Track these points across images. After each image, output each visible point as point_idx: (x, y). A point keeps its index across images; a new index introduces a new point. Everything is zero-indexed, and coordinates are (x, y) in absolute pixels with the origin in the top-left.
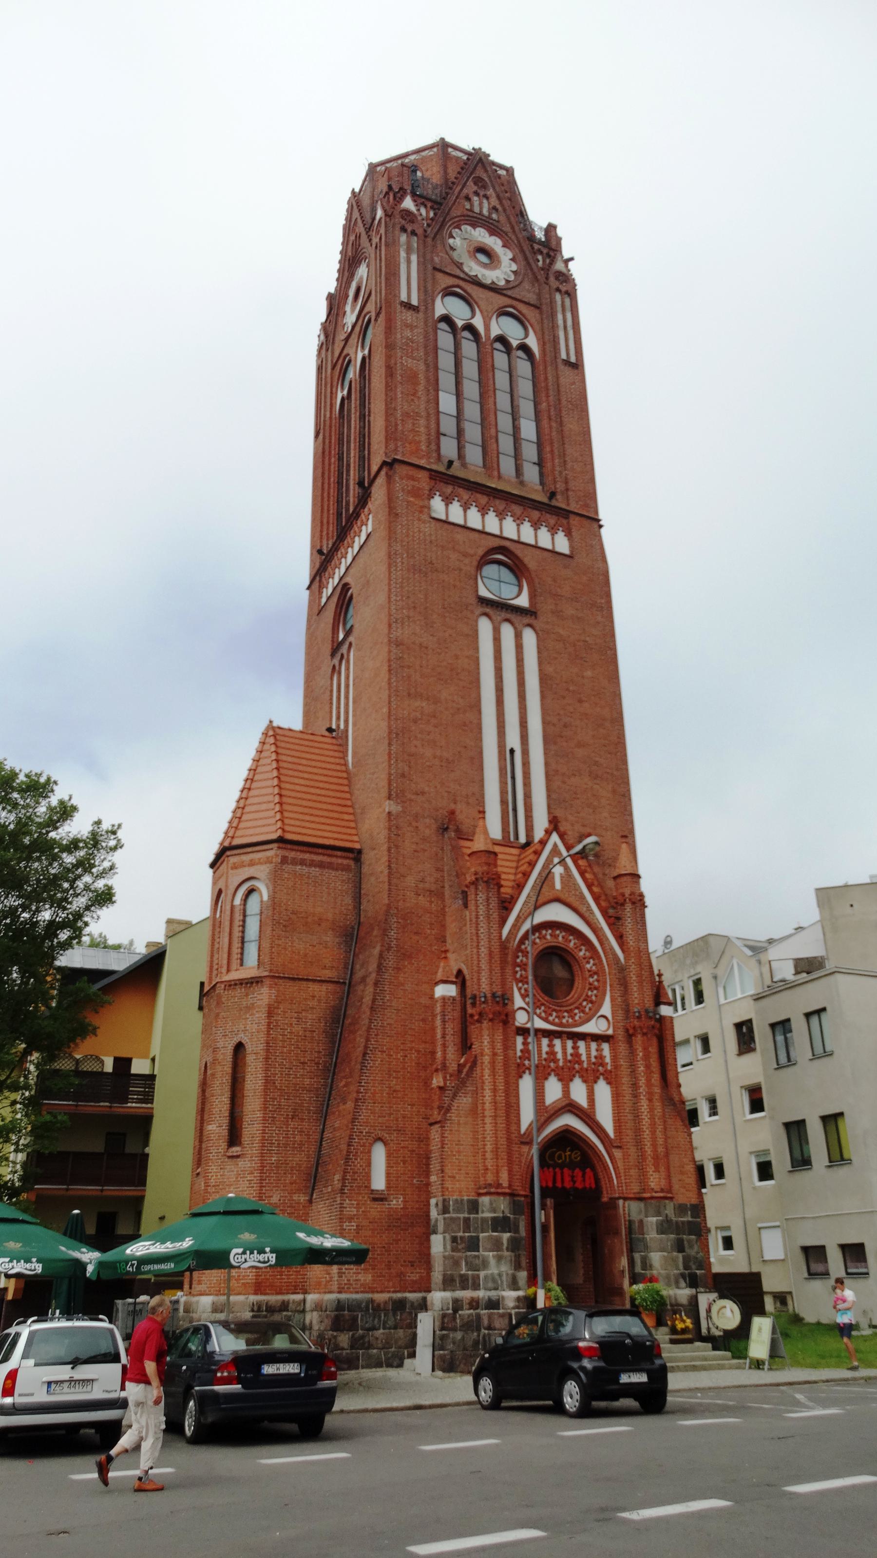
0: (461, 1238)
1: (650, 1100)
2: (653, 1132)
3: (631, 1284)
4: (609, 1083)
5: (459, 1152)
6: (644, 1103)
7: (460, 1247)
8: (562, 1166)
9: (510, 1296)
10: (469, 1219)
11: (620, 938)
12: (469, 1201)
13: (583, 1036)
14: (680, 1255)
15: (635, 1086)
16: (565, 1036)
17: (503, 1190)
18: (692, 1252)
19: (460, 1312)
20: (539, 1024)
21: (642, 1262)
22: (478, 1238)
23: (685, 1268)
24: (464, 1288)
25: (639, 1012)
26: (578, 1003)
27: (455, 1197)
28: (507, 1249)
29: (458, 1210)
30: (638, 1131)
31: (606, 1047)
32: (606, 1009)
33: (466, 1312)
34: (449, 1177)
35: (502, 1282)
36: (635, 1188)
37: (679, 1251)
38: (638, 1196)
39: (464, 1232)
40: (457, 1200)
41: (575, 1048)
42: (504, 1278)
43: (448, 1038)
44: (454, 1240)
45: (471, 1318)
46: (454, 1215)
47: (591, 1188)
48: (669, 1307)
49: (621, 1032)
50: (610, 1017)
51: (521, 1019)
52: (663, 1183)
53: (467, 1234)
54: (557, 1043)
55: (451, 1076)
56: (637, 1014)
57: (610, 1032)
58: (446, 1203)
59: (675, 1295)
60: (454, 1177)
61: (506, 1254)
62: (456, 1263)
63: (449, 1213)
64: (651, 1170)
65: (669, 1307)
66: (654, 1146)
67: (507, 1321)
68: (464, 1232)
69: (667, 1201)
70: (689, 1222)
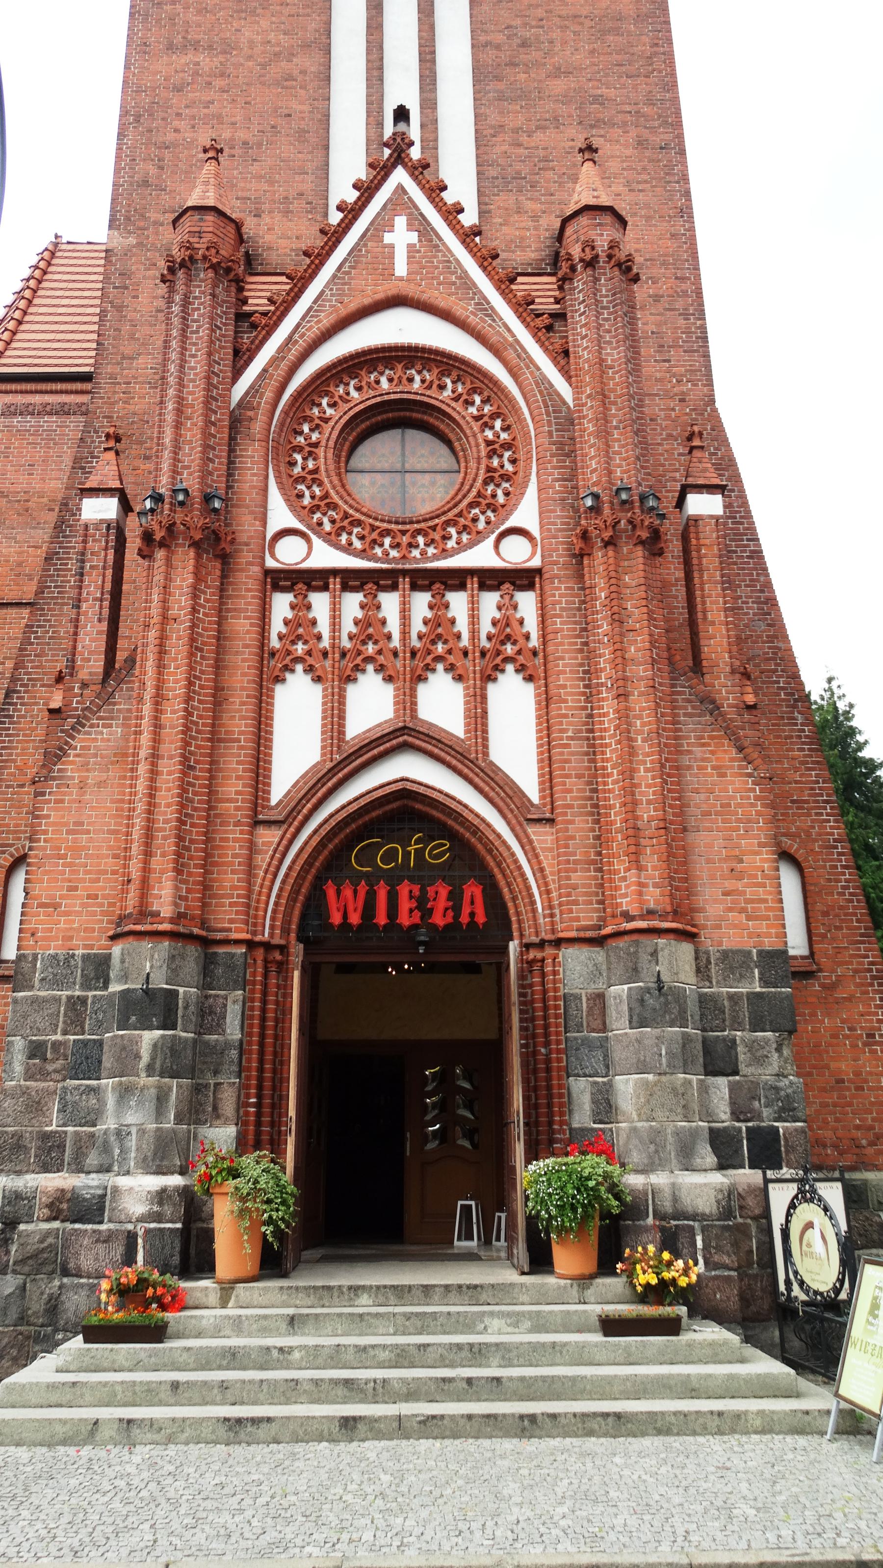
0: (56, 1045)
1: (622, 696)
2: (629, 773)
3: (528, 1162)
4: (529, 679)
5: (76, 850)
6: (609, 706)
7: (50, 1067)
8: (393, 879)
9: (137, 1190)
10: (83, 1000)
11: (562, 356)
12: (86, 958)
13: (457, 579)
14: (722, 1082)
15: (589, 673)
16: (405, 583)
17: (162, 927)
18: (766, 1074)
19: (22, 1227)
20: (325, 556)
21: (594, 1101)
22: (100, 1043)
23: (736, 1115)
24: (46, 1168)
25: (596, 496)
26: (456, 511)
27: (51, 952)
28: (150, 1070)
29: (56, 982)
30: (594, 778)
31: (527, 603)
32: (526, 513)
33: (35, 1228)
34: (41, 905)
35: (124, 1151)
36: (585, 916)
37: (712, 1070)
38: (589, 934)
39: (65, 1033)
40: (55, 957)
41: (439, 606)
42: (132, 1142)
43: (84, 606)
44: (36, 1050)
45: (50, 1240)
46: (42, 993)
47: (472, 924)
48: (650, 1220)
49: (560, 556)
50: (535, 532)
51: (290, 554)
52: (654, 897)
53: (72, 1038)
54: (390, 603)
55: (84, 685)
56: (589, 502)
57: (536, 562)
58: (26, 966)
59: (673, 1185)
60: (56, 906)
61: (144, 1080)
62: (35, 1107)
63: (31, 988)
64: (620, 865)
65: (650, 1220)
66: (631, 805)
67: (118, 1251)
68: (65, 1033)
69: (661, 942)
70: (754, 998)
